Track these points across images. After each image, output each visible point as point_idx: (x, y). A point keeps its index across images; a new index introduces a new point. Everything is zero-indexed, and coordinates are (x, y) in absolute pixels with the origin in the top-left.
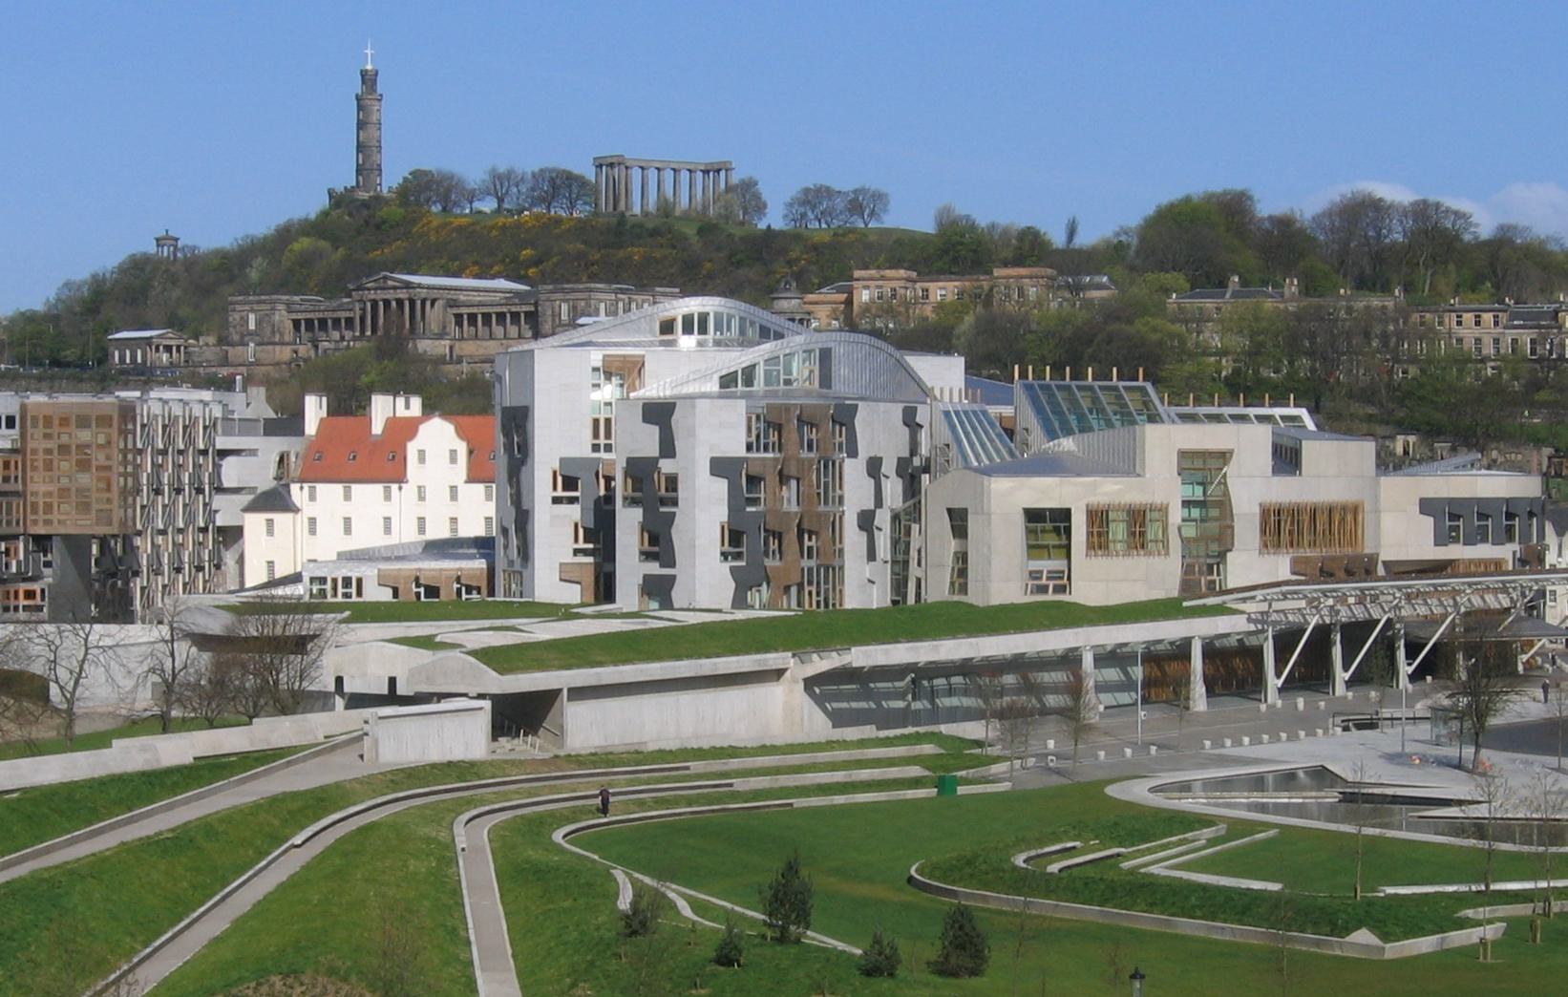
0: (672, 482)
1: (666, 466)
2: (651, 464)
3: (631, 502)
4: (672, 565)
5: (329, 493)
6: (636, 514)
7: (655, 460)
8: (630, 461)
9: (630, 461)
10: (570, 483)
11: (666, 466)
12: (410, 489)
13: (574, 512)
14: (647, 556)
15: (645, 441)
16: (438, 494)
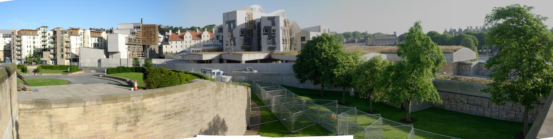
0: (274, 31)
1: (273, 28)
2: (270, 27)
3: (264, 34)
4: (275, 44)
5: (174, 42)
6: (267, 36)
7: (271, 27)
8: (265, 27)
9: (265, 27)
10: (242, 33)
11: (273, 28)
12: (184, 42)
13: (243, 37)
14: (268, 44)
15: (269, 24)
16: (188, 42)
